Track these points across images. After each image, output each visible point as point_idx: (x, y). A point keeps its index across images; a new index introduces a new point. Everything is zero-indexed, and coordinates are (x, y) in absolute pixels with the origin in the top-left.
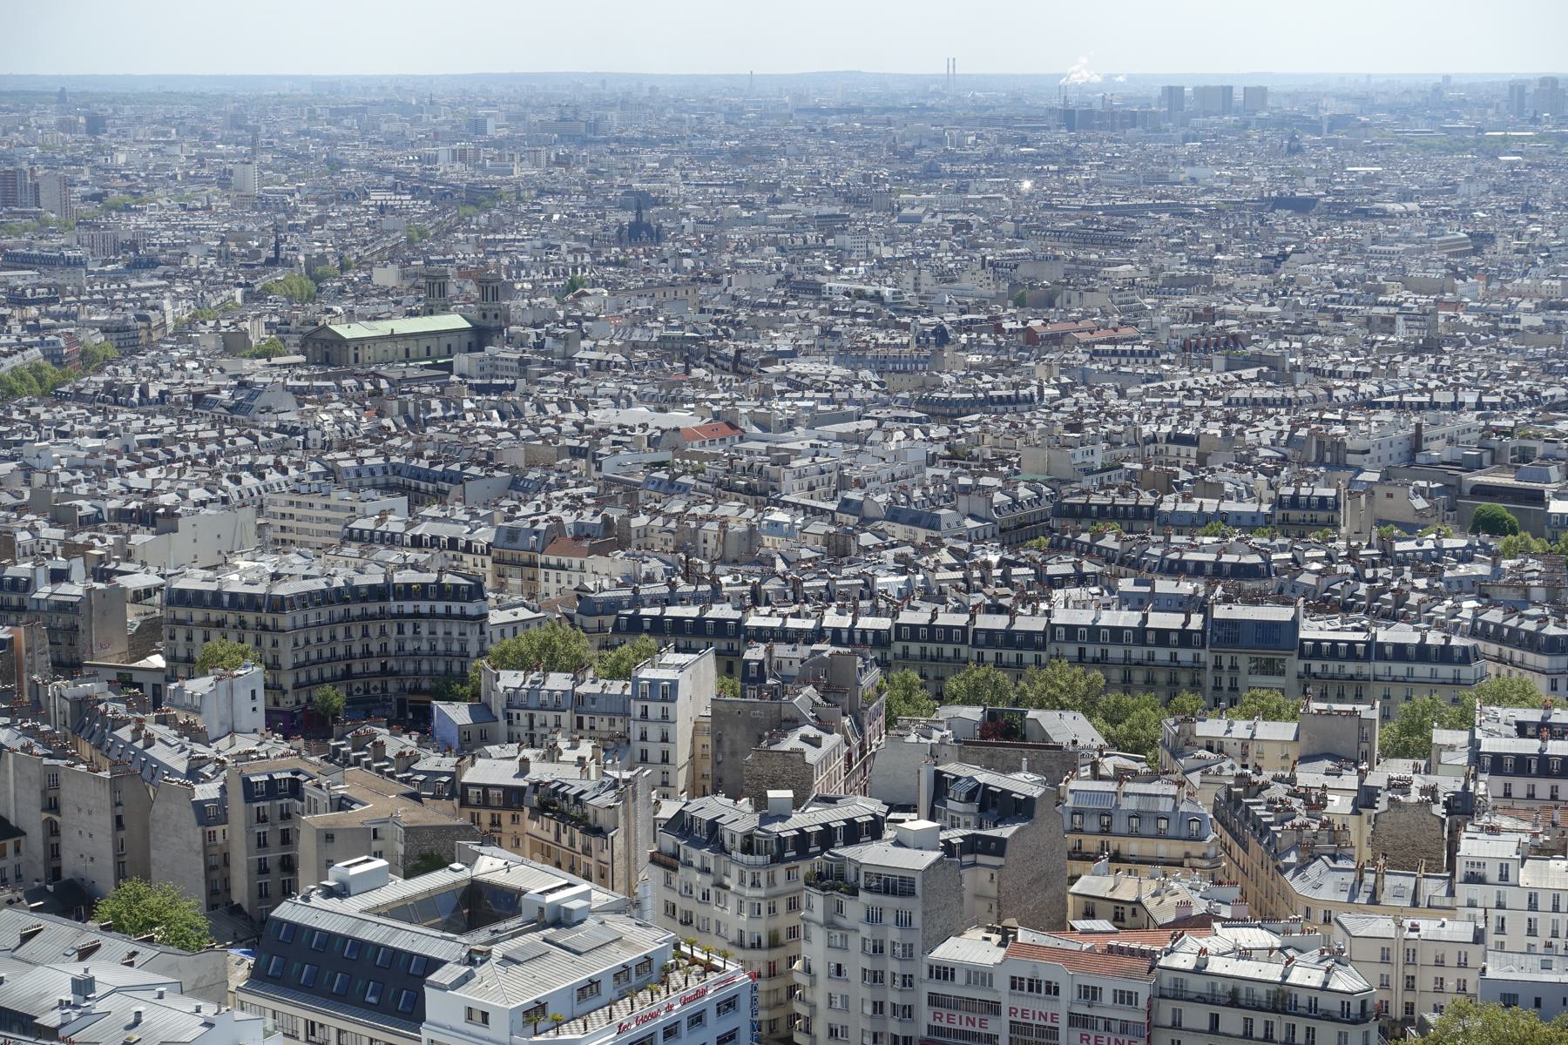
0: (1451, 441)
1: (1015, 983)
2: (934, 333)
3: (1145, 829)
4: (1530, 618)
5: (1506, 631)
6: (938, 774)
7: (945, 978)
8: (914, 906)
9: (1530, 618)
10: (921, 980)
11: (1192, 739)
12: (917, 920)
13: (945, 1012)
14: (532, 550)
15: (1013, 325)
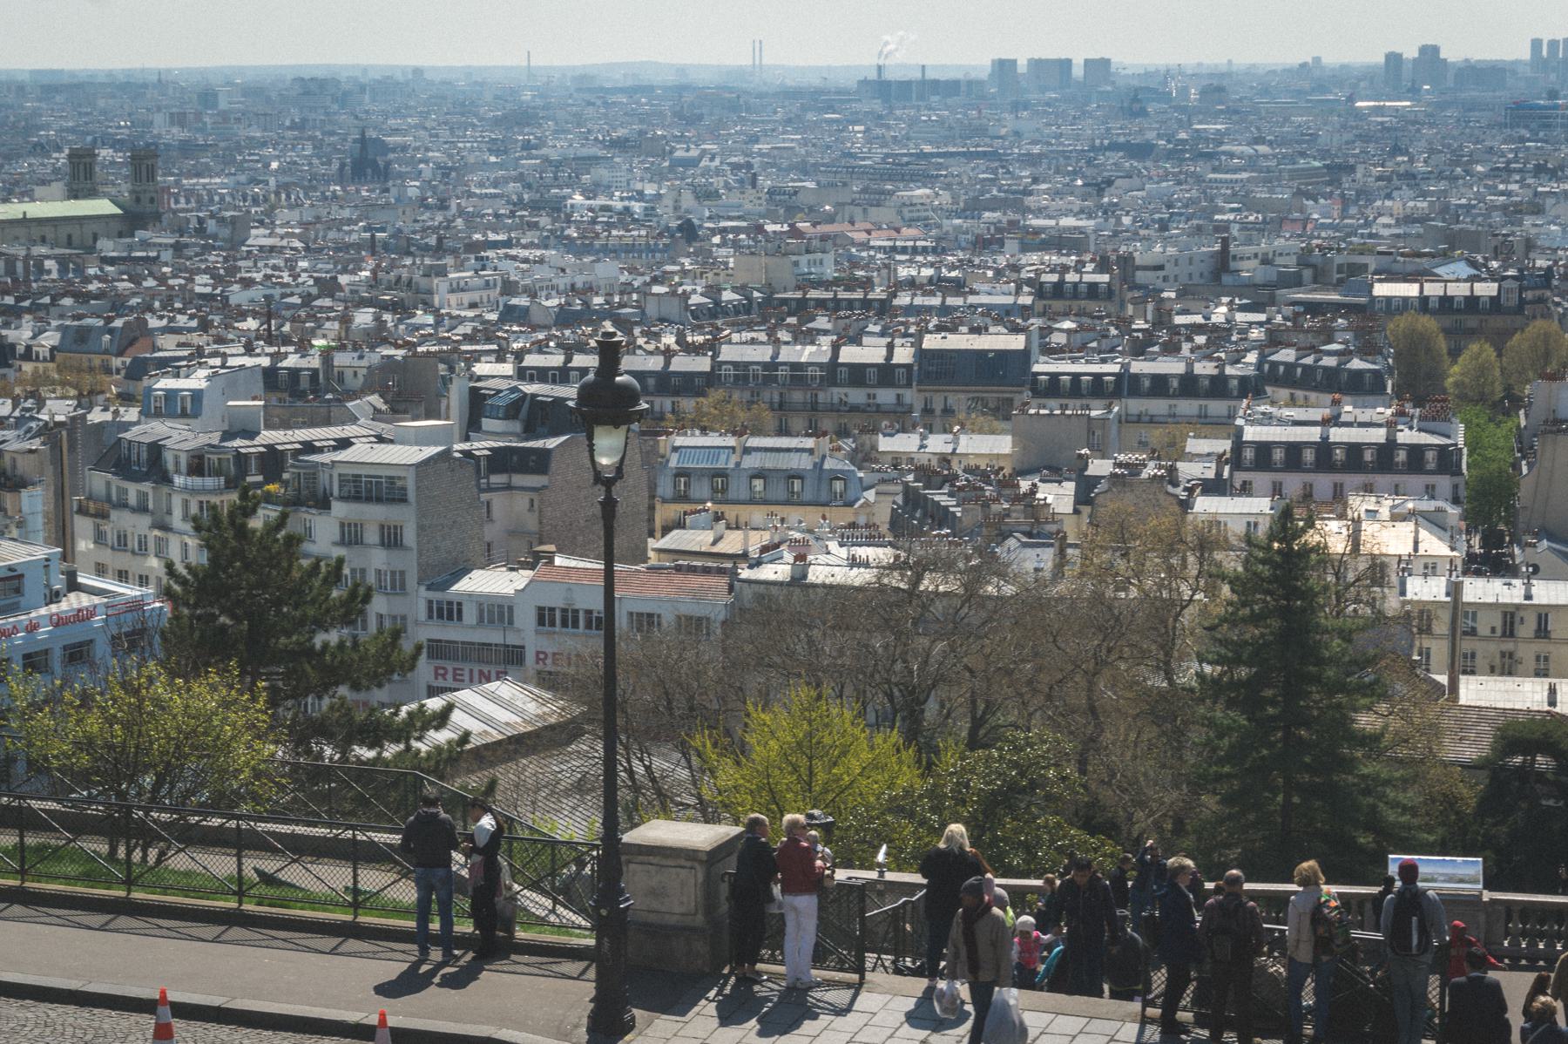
0: (1266, 261)
1: (544, 617)
2: (680, 228)
3: (771, 496)
4: (1330, 353)
5: (1299, 370)
6: (474, 392)
7: (450, 618)
8: (405, 518)
9: (1330, 353)
10: (417, 622)
11: (874, 454)
12: (410, 536)
13: (450, 666)
14: (106, 352)
15: (777, 228)
